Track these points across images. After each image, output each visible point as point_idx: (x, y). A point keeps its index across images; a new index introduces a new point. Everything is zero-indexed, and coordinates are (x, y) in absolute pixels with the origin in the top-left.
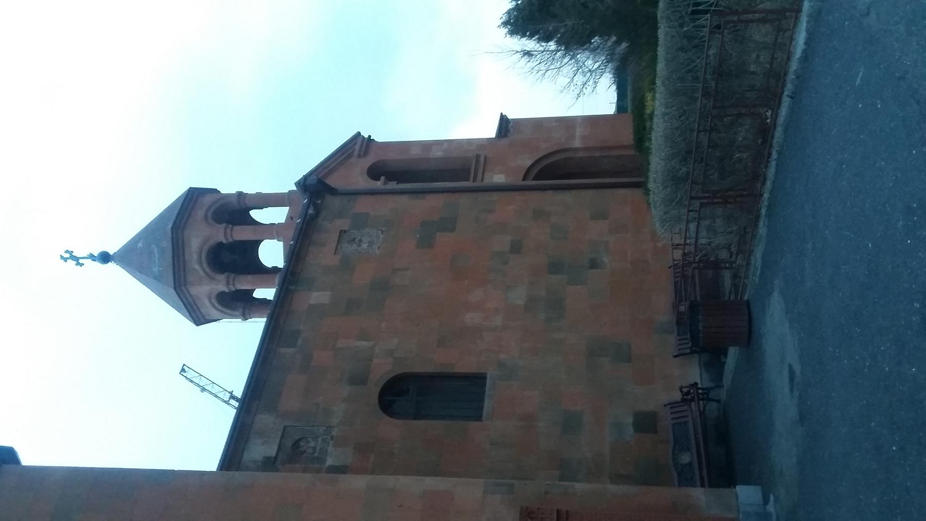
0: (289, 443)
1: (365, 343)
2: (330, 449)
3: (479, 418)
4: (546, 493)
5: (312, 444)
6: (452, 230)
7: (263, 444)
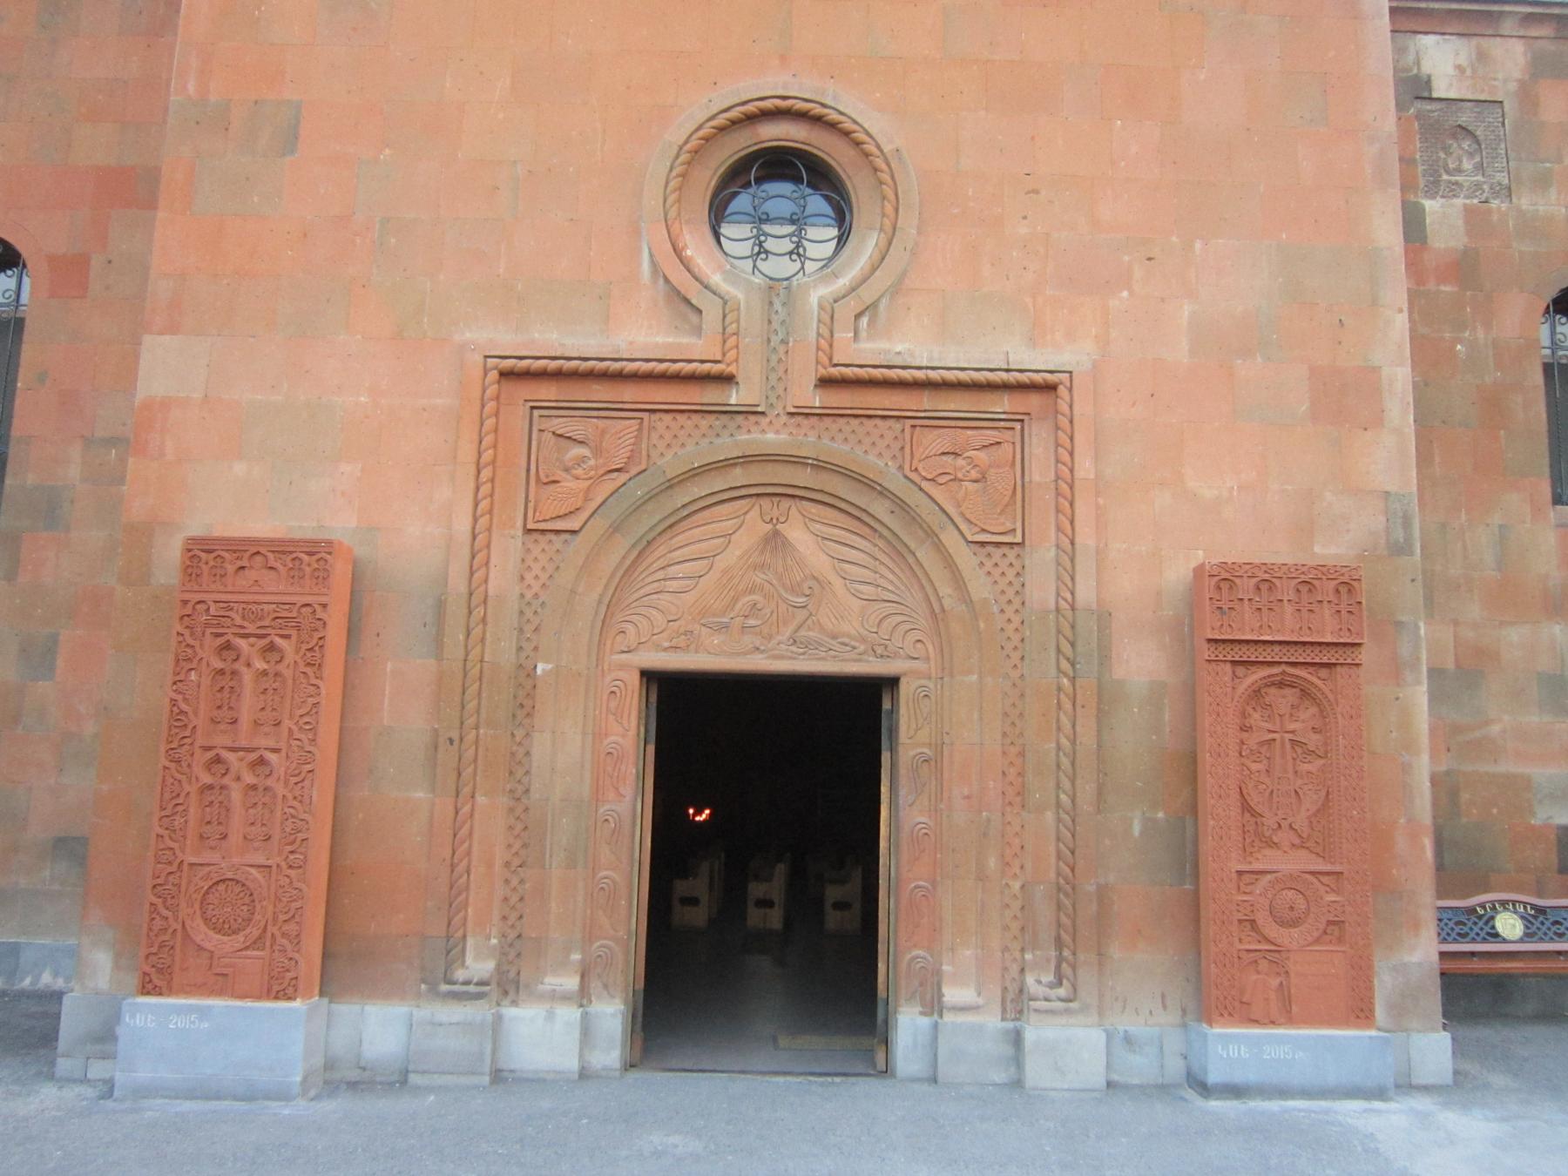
2: (1459, 202)
4: (1399, 624)
5: (1467, 165)
7: (1459, 68)
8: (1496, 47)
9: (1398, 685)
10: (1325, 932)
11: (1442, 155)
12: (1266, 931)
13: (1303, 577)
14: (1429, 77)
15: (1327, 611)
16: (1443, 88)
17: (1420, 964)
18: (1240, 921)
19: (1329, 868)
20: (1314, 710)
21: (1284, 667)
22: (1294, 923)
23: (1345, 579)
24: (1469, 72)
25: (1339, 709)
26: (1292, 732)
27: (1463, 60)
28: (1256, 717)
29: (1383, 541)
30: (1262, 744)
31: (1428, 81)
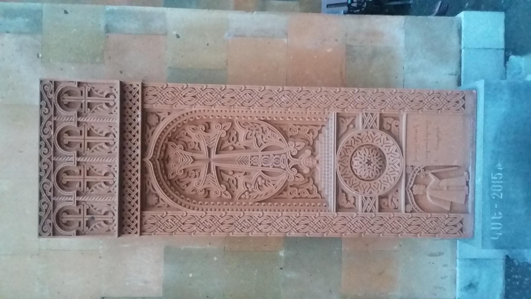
4: (108, 29)
9: (166, 34)
10: (389, 132)
12: (388, 187)
13: (54, 140)
15: (90, 120)
17: (407, 33)
18: (380, 209)
19: (332, 125)
20: (189, 130)
21: (147, 160)
22: (382, 158)
23: (53, 97)
25: (188, 110)
26: (209, 150)
28: (196, 184)
29: (28, 39)
30: (221, 180)
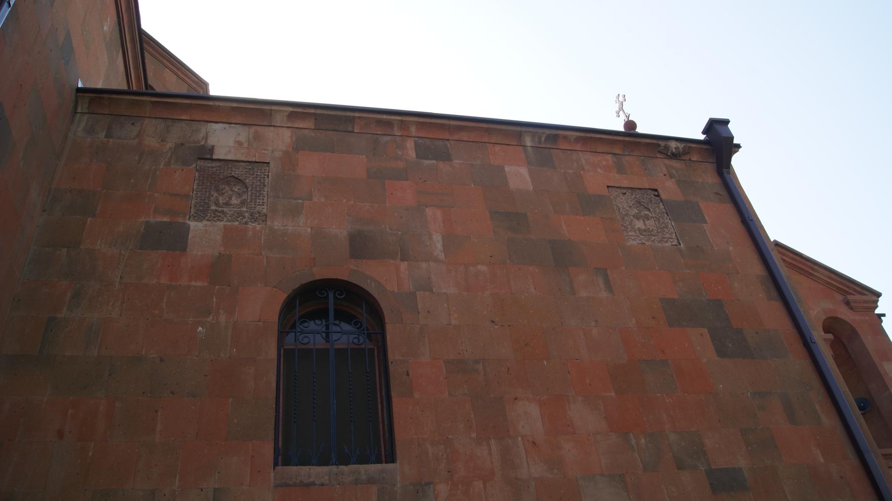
0: (236, 173)
1: (439, 246)
2: (221, 224)
3: (285, 456)
6: (722, 352)
8: (270, 133)
11: (215, 195)
14: (213, 146)
16: (219, 154)
24: (246, 145)
27: (242, 138)
31: (212, 150)
